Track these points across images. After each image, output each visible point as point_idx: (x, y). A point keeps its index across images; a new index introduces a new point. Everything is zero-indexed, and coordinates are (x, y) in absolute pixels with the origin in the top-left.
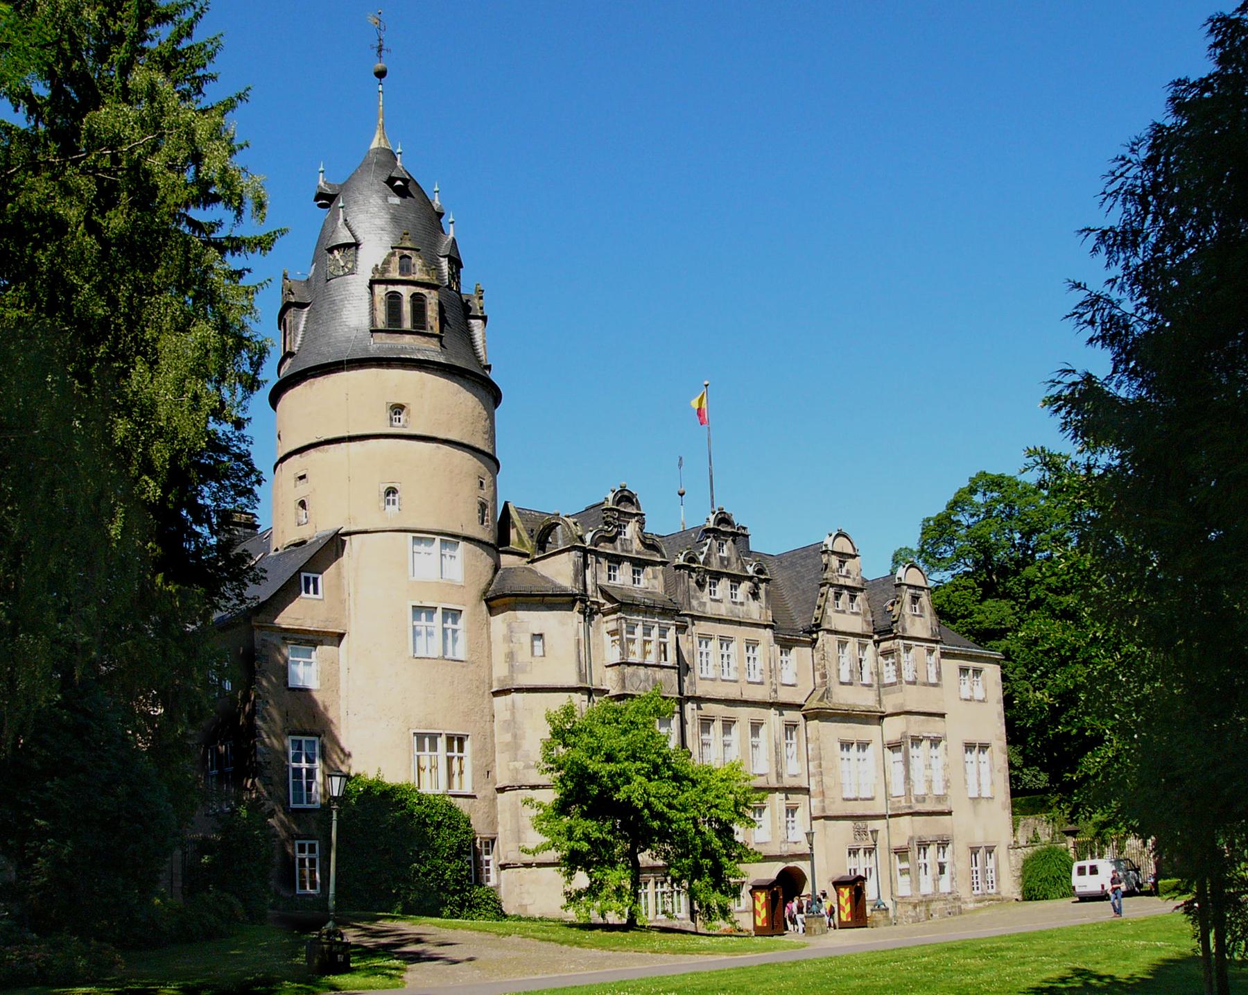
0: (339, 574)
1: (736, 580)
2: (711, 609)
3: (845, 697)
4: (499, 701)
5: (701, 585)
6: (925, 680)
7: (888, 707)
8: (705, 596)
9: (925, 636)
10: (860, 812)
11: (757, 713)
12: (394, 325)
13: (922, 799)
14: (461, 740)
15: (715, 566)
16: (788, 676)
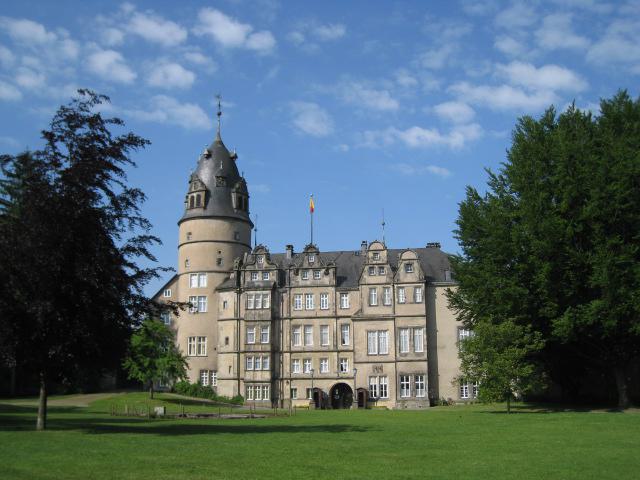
0: (177, 288)
1: (316, 270)
2: (301, 283)
3: (369, 311)
4: (220, 323)
5: (297, 274)
6: (412, 301)
7: (398, 313)
8: (299, 278)
9: (414, 280)
10: (379, 360)
11: (324, 322)
12: (192, 207)
13: (406, 355)
14: (204, 338)
15: (306, 265)
16: (346, 305)
